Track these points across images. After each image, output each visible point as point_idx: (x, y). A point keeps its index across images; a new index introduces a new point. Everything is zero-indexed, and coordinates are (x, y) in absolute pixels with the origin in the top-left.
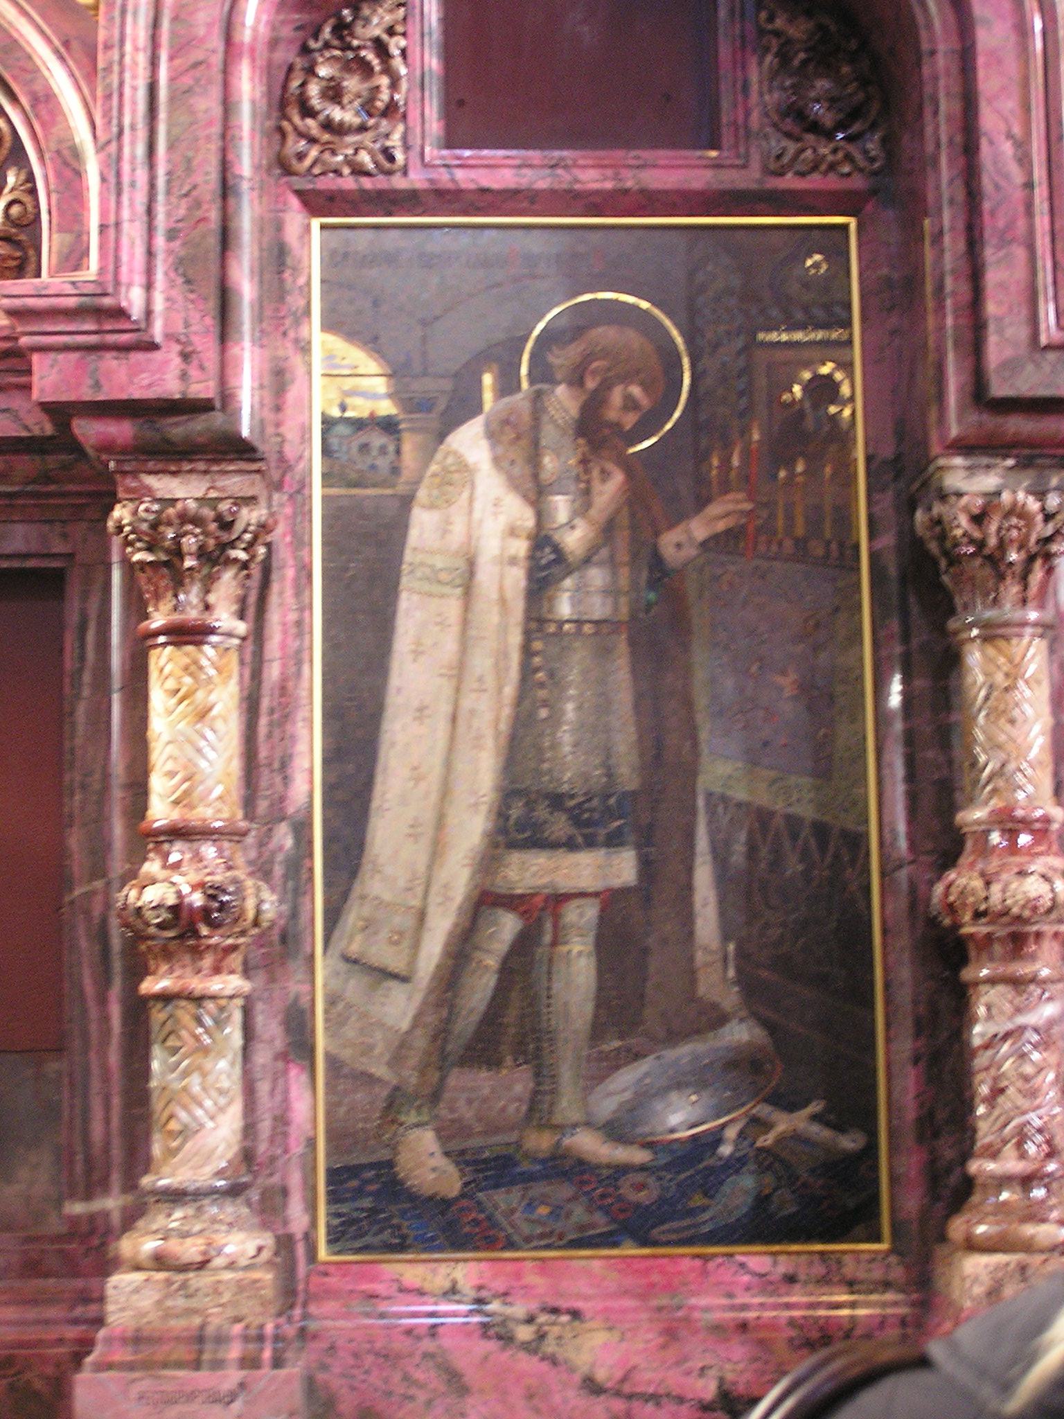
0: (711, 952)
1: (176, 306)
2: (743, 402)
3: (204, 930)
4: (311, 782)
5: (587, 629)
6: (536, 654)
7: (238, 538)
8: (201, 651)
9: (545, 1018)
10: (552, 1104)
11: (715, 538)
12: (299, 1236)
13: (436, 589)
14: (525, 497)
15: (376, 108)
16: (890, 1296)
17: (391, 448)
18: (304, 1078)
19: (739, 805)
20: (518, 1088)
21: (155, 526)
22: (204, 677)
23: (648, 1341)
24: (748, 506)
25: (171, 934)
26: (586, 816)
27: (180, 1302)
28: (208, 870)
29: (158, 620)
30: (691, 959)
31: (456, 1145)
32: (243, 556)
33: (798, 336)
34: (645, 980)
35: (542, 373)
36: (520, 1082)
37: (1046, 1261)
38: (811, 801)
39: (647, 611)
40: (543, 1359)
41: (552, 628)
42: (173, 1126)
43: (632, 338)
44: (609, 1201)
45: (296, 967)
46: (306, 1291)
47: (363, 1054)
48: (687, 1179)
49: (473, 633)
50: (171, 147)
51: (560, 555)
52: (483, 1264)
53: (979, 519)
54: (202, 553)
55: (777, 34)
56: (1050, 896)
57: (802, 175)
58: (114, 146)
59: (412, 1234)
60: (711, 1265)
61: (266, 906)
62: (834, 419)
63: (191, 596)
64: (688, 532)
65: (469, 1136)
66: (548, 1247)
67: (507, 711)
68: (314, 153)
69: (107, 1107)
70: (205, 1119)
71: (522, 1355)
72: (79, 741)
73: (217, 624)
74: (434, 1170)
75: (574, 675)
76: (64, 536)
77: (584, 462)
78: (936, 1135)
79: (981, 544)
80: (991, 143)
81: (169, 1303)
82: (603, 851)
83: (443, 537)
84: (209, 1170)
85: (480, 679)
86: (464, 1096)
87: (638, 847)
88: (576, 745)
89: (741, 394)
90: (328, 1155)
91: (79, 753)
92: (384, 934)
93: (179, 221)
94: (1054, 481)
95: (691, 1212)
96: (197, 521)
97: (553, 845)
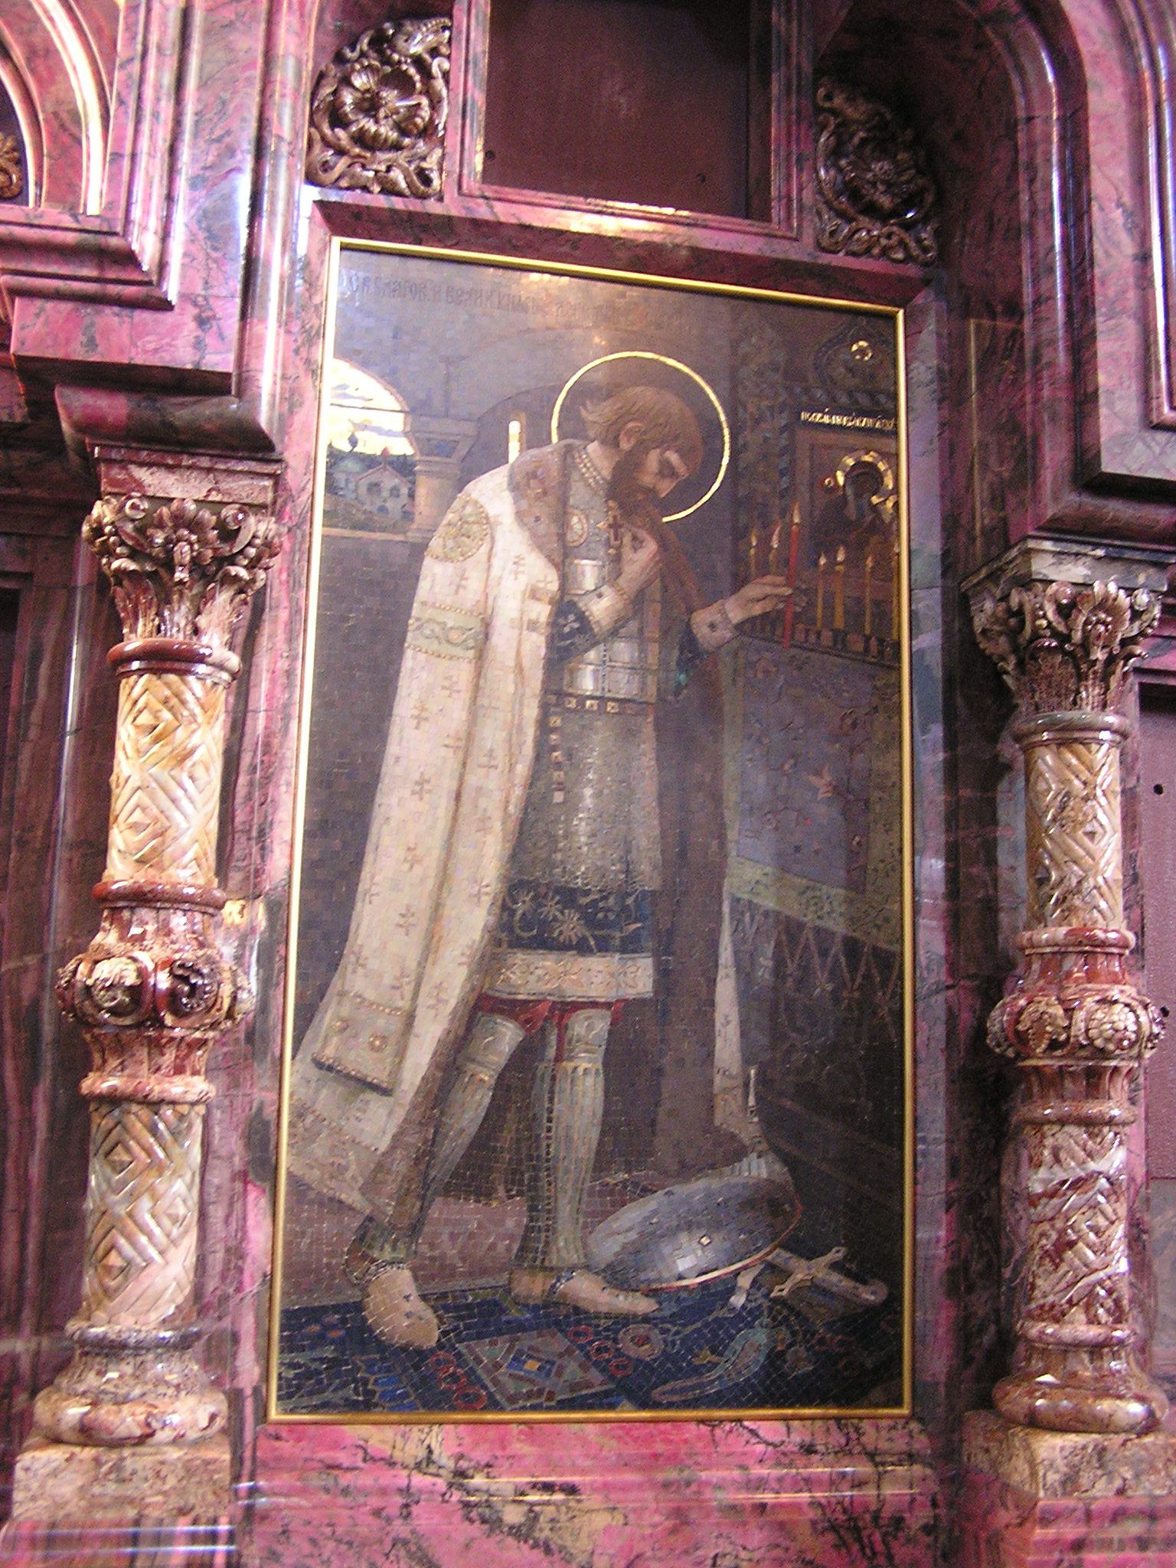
0: (731, 1077)
1: (195, 263)
2: (785, 482)
3: (169, 1020)
4: (291, 856)
6: (554, 730)
7: (241, 552)
8: (185, 682)
9: (544, 1144)
10: (547, 1243)
11: (751, 620)
12: (248, 1391)
14: (549, 558)
15: (415, 125)
16: (918, 1469)
17: (404, 491)
18: (264, 1202)
19: (766, 914)
20: (510, 1223)
21: (141, 530)
22: (186, 713)
23: (655, 1526)
24: (788, 591)
25: (128, 1021)
27: (112, 1488)
28: (176, 947)
29: (133, 643)
31: (436, 1287)
32: (244, 574)
33: (837, 420)
34: (657, 1104)
35: (572, 426)
36: (512, 1217)
37: (1124, 1444)
38: (841, 914)
39: (677, 694)
40: (535, 1546)
41: (573, 703)
42: (114, 1259)
43: (674, 404)
44: (606, 1356)
45: (263, 1071)
46: (254, 1458)
47: (332, 1177)
48: (694, 1331)
50: (203, 85)
51: (584, 622)
52: (462, 1427)
53: (1065, 611)
54: (196, 564)
55: (834, 112)
56: (1135, 1028)
57: (854, 254)
58: (137, 65)
59: (379, 1389)
60: (718, 1431)
61: (243, 995)
62: (874, 508)
63: (179, 616)
64: (723, 612)
65: (452, 1276)
66: (535, 1408)
67: (518, 792)
68: (342, 164)
69: (23, 1229)
70: (152, 1252)
71: (510, 1541)
72: (21, 789)
73: (207, 652)
74: (408, 1315)
75: (594, 758)
76: (23, 553)
77: (615, 526)
78: (970, 1289)
79: (1065, 638)
80: (1102, 209)
81: (97, 1489)
82: (617, 956)
83: (457, 592)
84: (154, 1317)
85: (490, 754)
87: (656, 955)
88: (593, 835)
89: (782, 474)
90: (285, 1294)
91: (19, 804)
92: (365, 1038)
93: (205, 168)
94: (1141, 579)
95: (697, 1371)
96: (195, 525)
97: (563, 947)
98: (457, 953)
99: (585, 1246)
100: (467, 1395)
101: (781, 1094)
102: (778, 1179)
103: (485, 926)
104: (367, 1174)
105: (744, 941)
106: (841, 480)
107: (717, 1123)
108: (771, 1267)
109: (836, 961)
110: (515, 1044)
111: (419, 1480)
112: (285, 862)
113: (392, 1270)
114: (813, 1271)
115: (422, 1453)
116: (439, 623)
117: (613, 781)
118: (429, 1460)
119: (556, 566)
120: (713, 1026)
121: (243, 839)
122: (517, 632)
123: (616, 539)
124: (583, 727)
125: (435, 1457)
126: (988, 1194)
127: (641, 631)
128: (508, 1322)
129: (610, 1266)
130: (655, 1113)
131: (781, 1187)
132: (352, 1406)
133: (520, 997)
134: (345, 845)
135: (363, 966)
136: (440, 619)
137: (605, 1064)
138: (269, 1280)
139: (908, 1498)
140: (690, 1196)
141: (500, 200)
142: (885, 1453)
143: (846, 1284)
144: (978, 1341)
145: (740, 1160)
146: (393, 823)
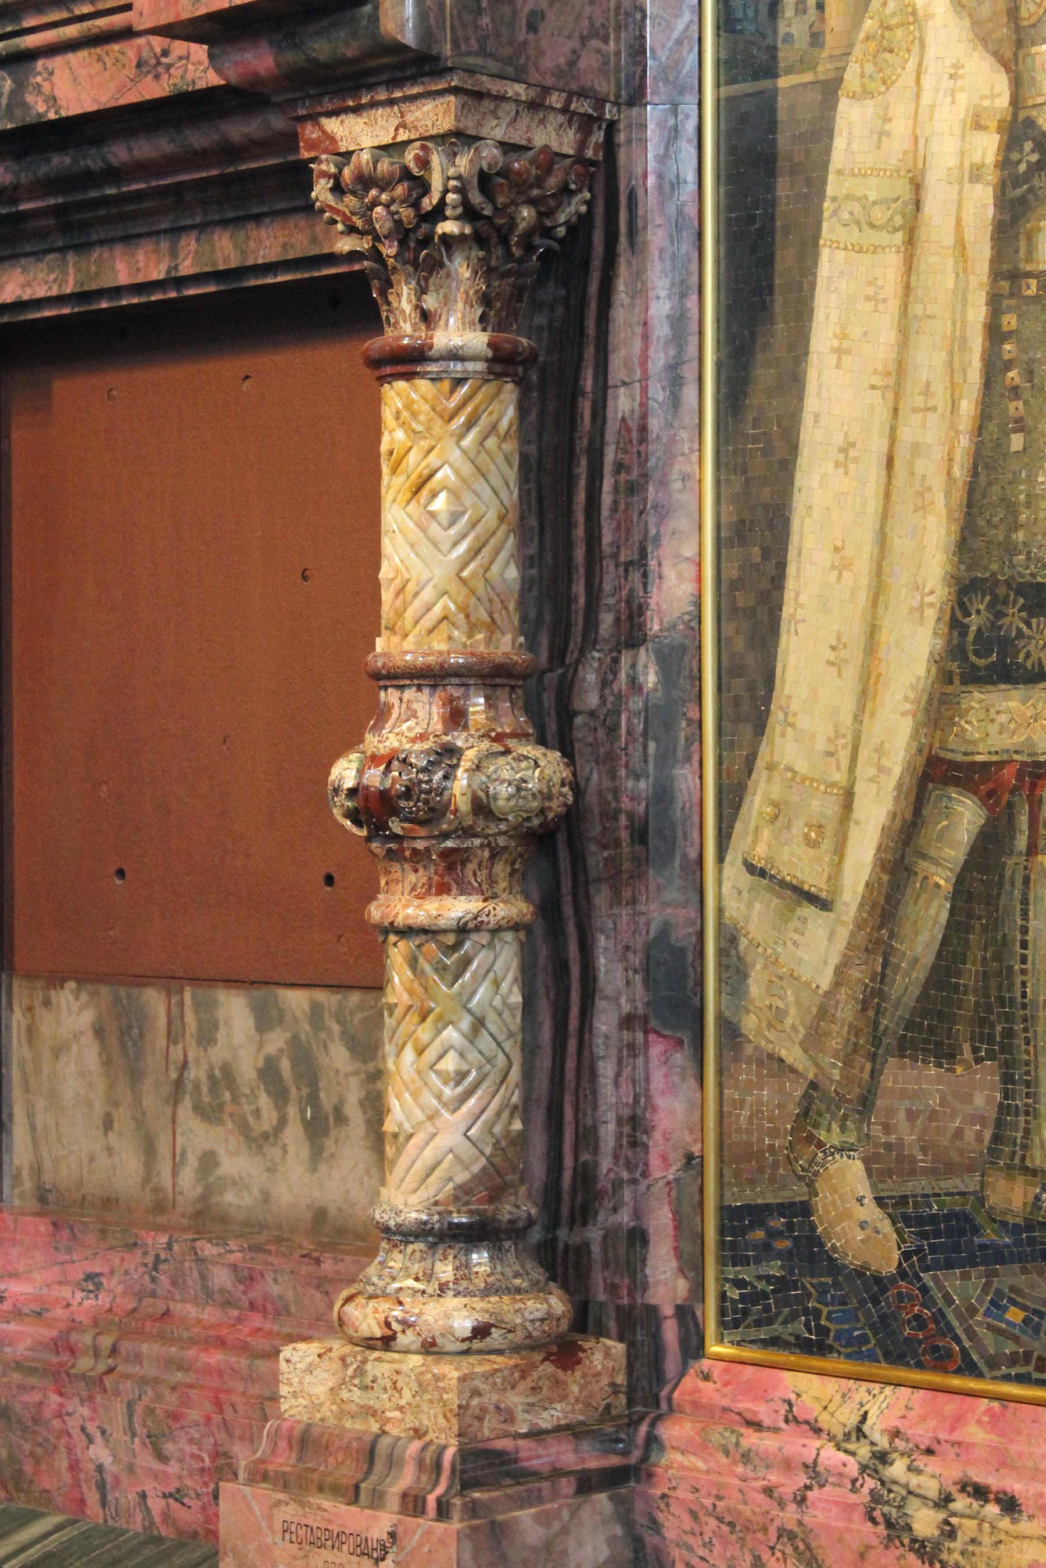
4: (699, 580)
9: (1018, 979)
10: (1027, 1132)
12: (668, 1310)
20: (979, 1100)
31: (893, 1188)
47: (770, 1026)
49: (917, 309)
65: (912, 1173)
66: (1021, 1379)
67: (964, 442)
74: (863, 1225)
83: (878, 146)
85: (927, 390)
86: (906, 1104)
92: (798, 828)
98: (899, 697)
100: (935, 1349)
103: (931, 653)
104: (808, 1020)
110: (975, 830)
111: (831, 1455)
112: (689, 588)
116: (858, 199)
118: (859, 1432)
119: (1005, 65)
121: (612, 568)
122: (956, 188)
128: (983, 1247)
132: (806, 1347)
133: (979, 758)
134: (765, 555)
135: (792, 725)
136: (858, 194)
138: (692, 1162)
146: (816, 514)
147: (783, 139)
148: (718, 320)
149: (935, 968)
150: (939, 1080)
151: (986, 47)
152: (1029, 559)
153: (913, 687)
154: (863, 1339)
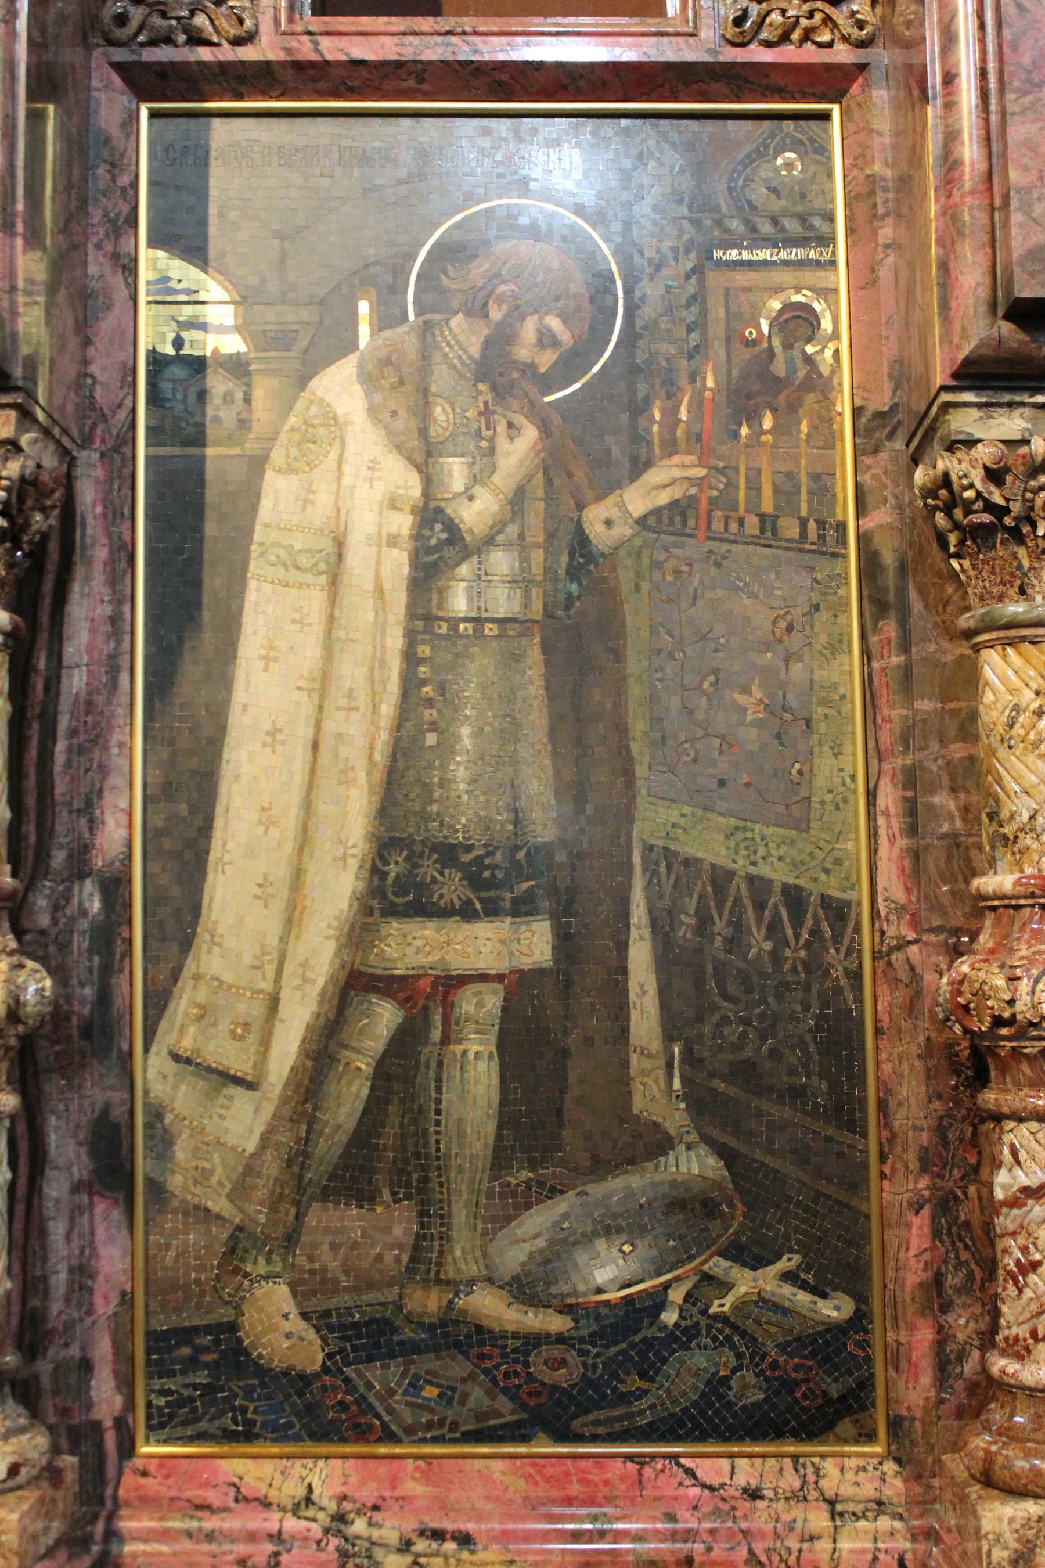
0: (650, 1056)
5: (490, 629)
6: (422, 661)
9: (433, 1139)
10: (441, 1253)
11: (657, 512)
13: (294, 576)
14: (410, 459)
16: (885, 1523)
17: (239, 395)
20: (398, 1231)
24: (701, 472)
26: (487, 874)
30: (626, 1063)
34: (563, 1092)
47: (196, 1183)
52: (352, 1461)
59: (259, 1419)
60: (648, 1471)
65: (336, 1291)
67: (384, 737)
74: (288, 1336)
75: (471, 691)
77: (486, 412)
82: (509, 920)
83: (303, 510)
85: (350, 694)
86: (330, 1238)
87: (555, 918)
88: (474, 781)
92: (225, 1025)
97: (444, 913)
98: (324, 925)
99: (485, 1255)
100: (357, 1426)
101: (712, 1074)
102: (710, 1174)
104: (234, 1177)
105: (661, 897)
106: (765, 329)
107: (635, 1111)
108: (707, 1278)
109: (777, 915)
110: (393, 1026)
113: (267, 1286)
114: (761, 1282)
115: (301, 1492)
116: (284, 547)
117: (494, 716)
119: (417, 467)
120: (627, 997)
122: (374, 550)
123: (488, 428)
124: (457, 655)
125: (315, 1497)
126: (965, 1193)
127: (521, 536)
128: (401, 1343)
129: (516, 1278)
130: (562, 1101)
131: (716, 1185)
132: (229, 1436)
134: (193, 809)
135: (220, 945)
137: (501, 1045)
138: (126, 1299)
139: (870, 1556)
140: (608, 1196)
141: (328, 34)
142: (848, 1500)
143: (803, 1297)
144: (958, 1370)
145: (665, 1154)
147: (211, 495)
148: (146, 625)
149: (356, 1132)
150: (360, 1218)
151: (400, 452)
152: (442, 824)
153: (336, 918)
154: (290, 1425)
